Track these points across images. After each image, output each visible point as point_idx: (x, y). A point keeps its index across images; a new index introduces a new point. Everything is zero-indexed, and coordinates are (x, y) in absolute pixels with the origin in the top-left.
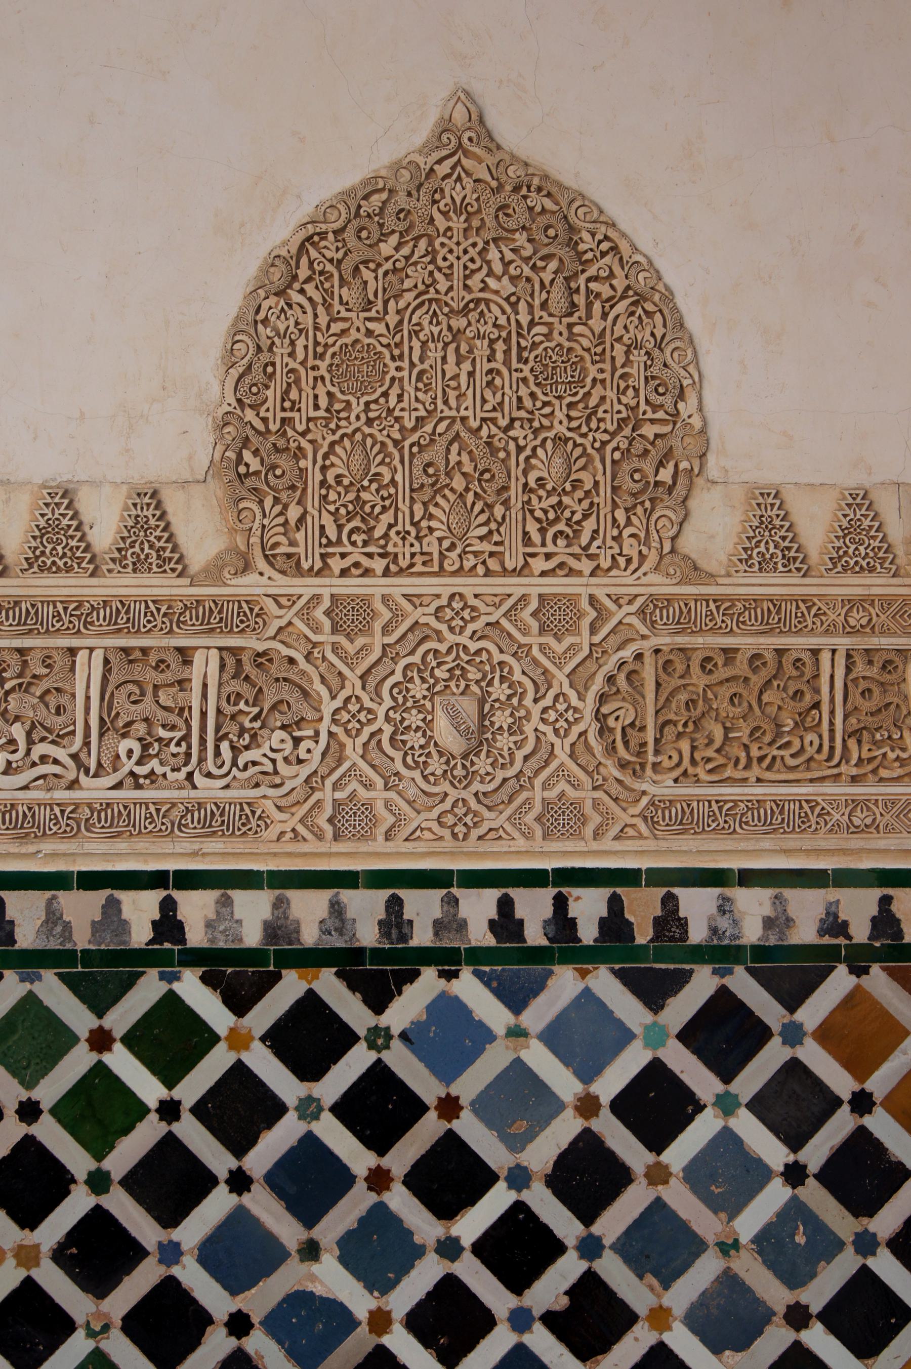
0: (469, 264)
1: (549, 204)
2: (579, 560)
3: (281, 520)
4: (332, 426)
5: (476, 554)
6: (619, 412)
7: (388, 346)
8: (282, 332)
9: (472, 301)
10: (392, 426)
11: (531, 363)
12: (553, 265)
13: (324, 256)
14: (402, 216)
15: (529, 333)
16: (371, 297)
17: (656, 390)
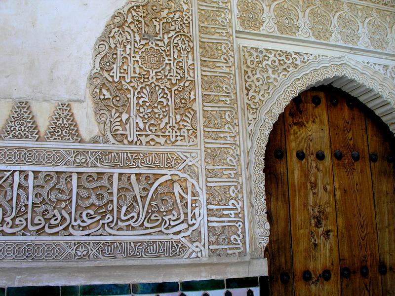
3: (119, 119)
4: (142, 81)
10: (167, 82)
13: (138, 14)
16: (158, 32)
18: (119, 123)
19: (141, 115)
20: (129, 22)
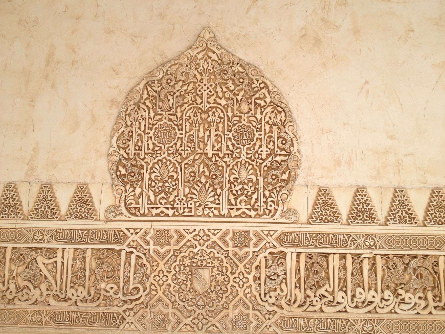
0: (209, 93)
1: (241, 69)
3: (133, 193)
4: (154, 156)
5: (210, 208)
6: (267, 151)
7: (177, 125)
8: (136, 119)
9: (210, 107)
11: (233, 132)
12: (242, 93)
13: (153, 90)
14: (184, 74)
15: (232, 120)
16: (171, 106)
17: (282, 142)
18: (132, 197)
19: (153, 189)
20: (144, 98)
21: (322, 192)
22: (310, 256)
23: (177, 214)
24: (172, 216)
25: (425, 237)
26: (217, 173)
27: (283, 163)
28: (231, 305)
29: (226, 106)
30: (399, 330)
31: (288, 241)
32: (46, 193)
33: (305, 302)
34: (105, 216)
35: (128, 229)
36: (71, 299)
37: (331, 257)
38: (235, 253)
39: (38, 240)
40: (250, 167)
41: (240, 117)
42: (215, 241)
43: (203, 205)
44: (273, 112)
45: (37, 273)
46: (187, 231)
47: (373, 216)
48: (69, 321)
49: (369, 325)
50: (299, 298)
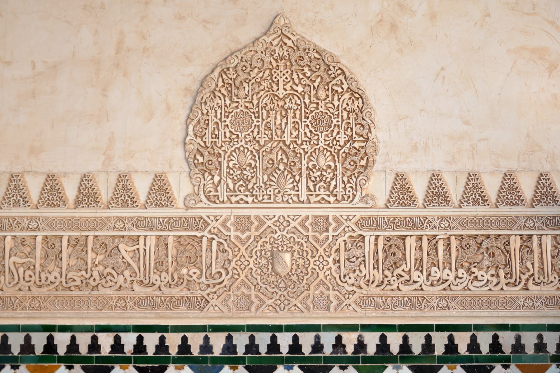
0: (285, 80)
1: (317, 56)
2: (329, 197)
3: (212, 181)
6: (345, 138)
8: (212, 107)
9: (286, 94)
10: (255, 144)
11: (310, 119)
13: (228, 77)
14: (259, 61)
16: (247, 93)
18: (211, 185)
19: (231, 177)
21: (399, 177)
22: (388, 239)
23: (256, 201)
24: (251, 203)
25: (498, 218)
26: (295, 160)
27: (361, 149)
28: (312, 287)
29: (303, 93)
30: (472, 305)
31: (367, 225)
32: (125, 182)
33: (383, 282)
34: (185, 204)
35: (208, 217)
36: (155, 285)
37: (408, 238)
38: (315, 238)
39: (119, 228)
40: (328, 154)
41: (318, 104)
42: (295, 227)
43: (282, 192)
44: (350, 98)
45: (120, 260)
46: (267, 217)
47: (448, 199)
48: (153, 306)
49: (444, 302)
50: (377, 278)
